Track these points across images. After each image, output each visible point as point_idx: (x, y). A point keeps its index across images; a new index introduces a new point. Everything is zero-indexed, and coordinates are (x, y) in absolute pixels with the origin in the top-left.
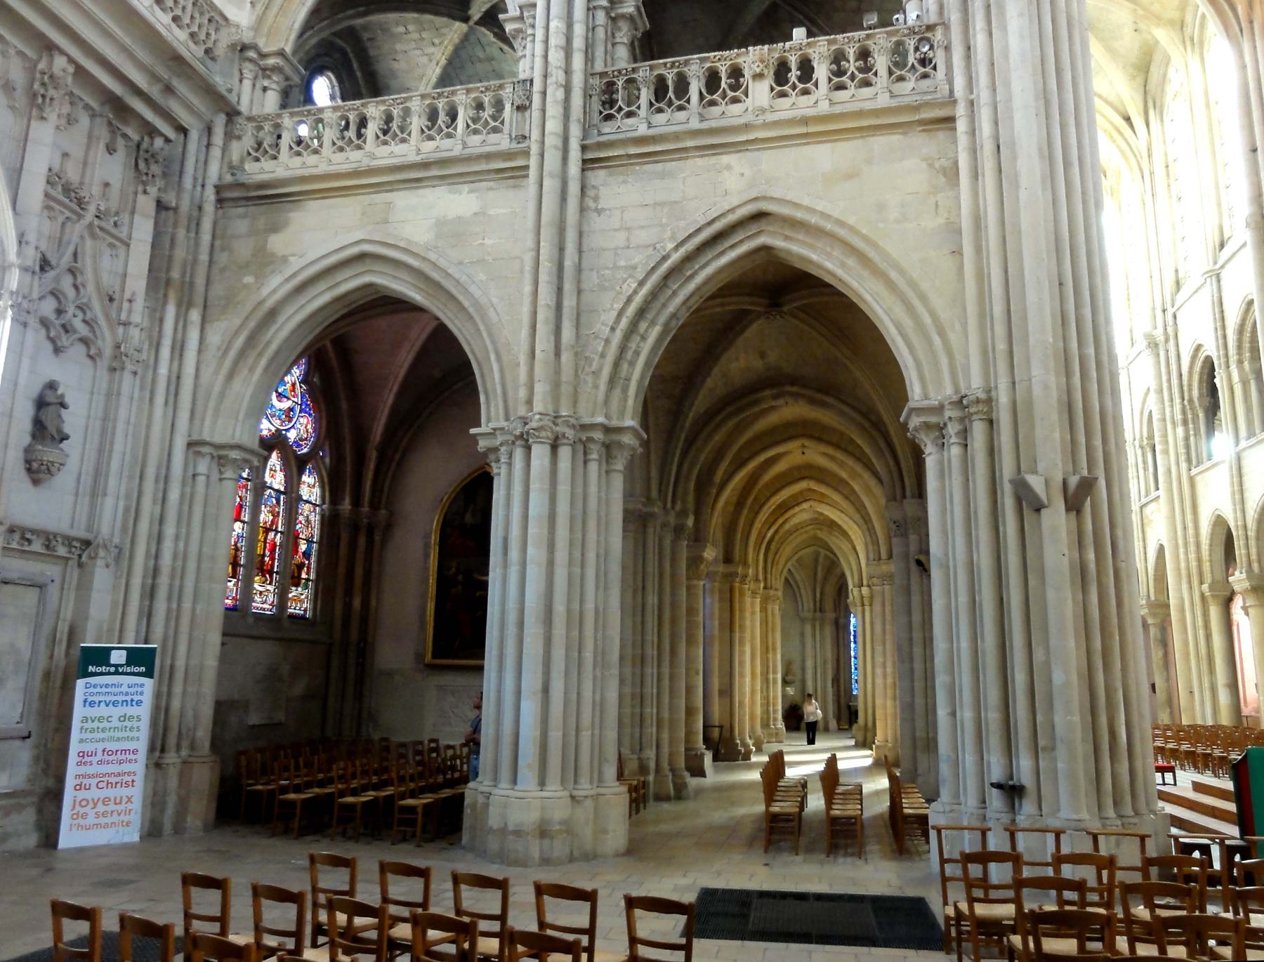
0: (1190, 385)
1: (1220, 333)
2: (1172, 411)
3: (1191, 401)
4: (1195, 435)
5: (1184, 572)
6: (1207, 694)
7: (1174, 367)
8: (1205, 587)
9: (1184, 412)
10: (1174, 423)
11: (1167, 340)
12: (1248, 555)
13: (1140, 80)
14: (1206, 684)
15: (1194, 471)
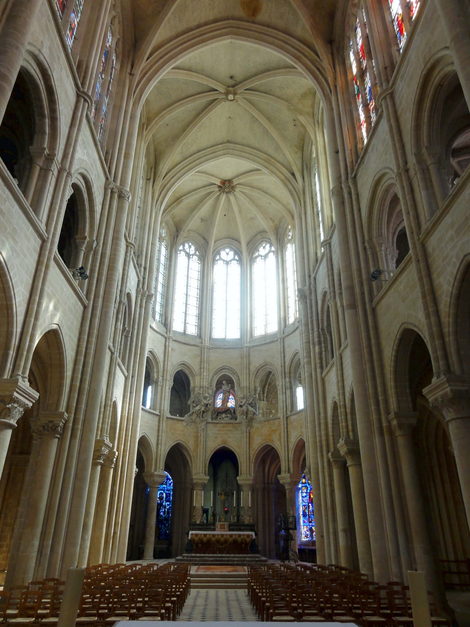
0: (322, 320)
1: (331, 277)
2: (313, 337)
3: (323, 329)
4: (325, 351)
5: (318, 444)
6: (332, 537)
7: (314, 309)
8: (330, 454)
9: (319, 337)
10: (314, 344)
11: (311, 293)
12: (347, 426)
13: (299, 154)
14: (331, 530)
15: (324, 373)
